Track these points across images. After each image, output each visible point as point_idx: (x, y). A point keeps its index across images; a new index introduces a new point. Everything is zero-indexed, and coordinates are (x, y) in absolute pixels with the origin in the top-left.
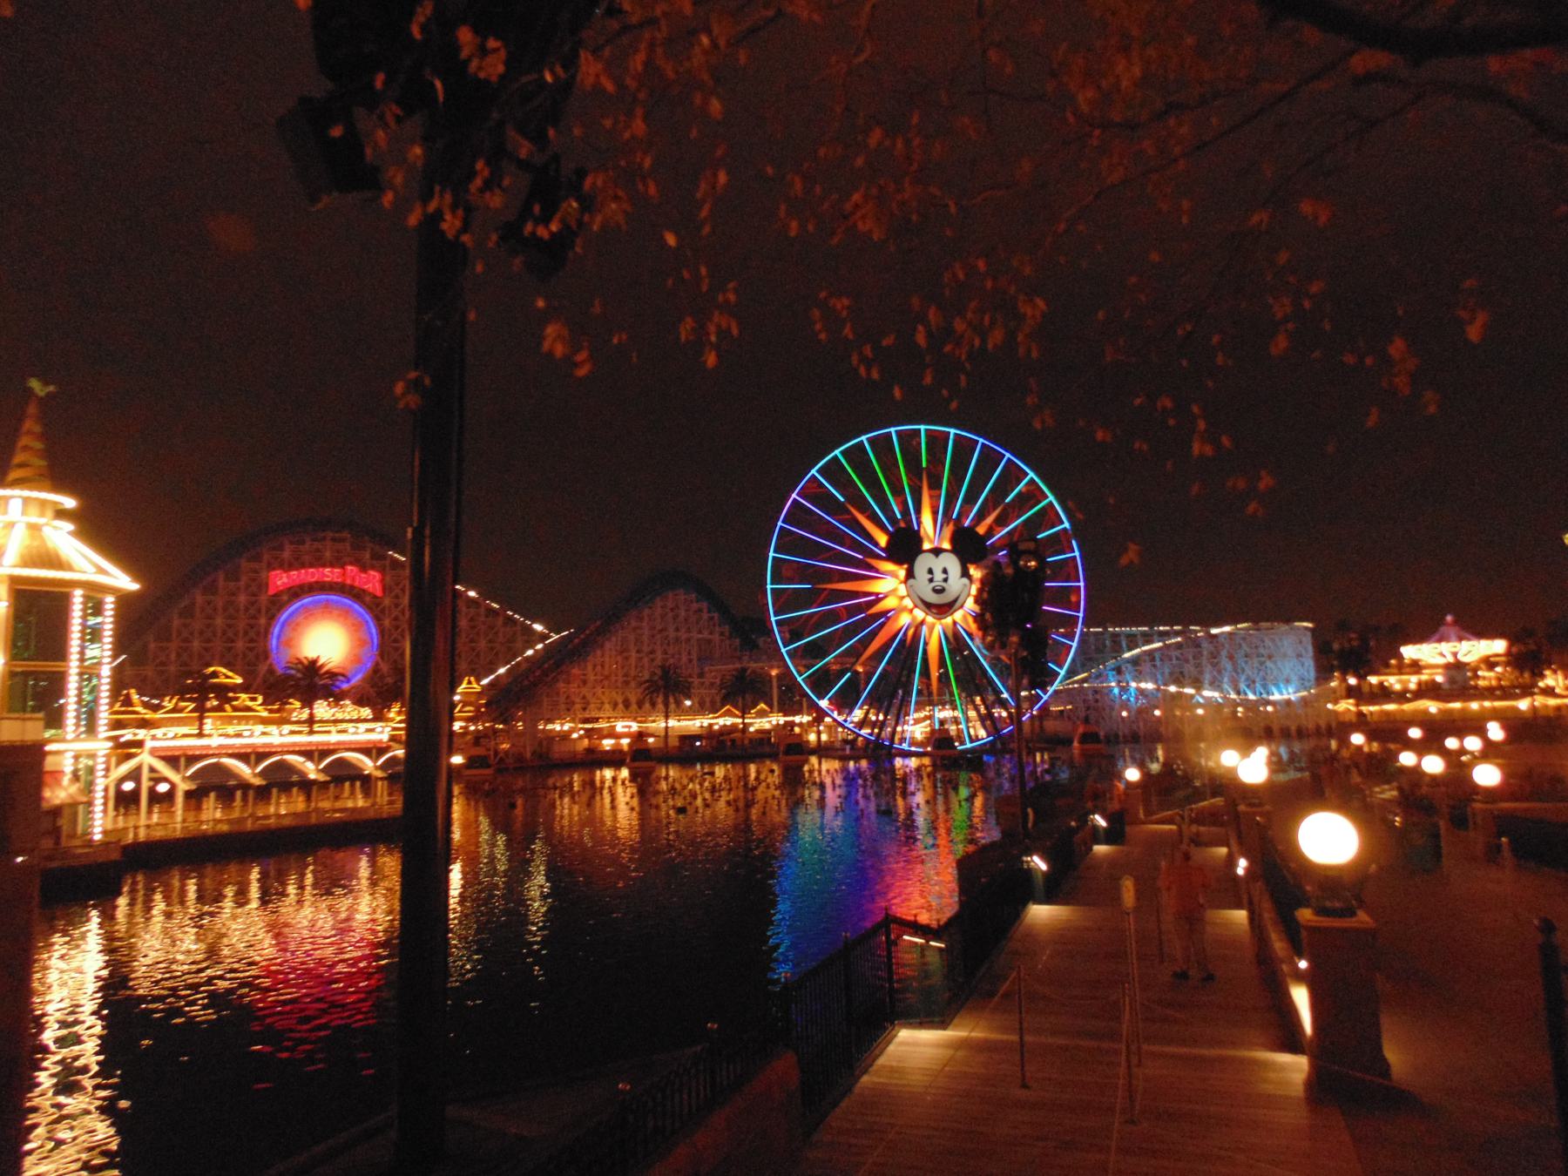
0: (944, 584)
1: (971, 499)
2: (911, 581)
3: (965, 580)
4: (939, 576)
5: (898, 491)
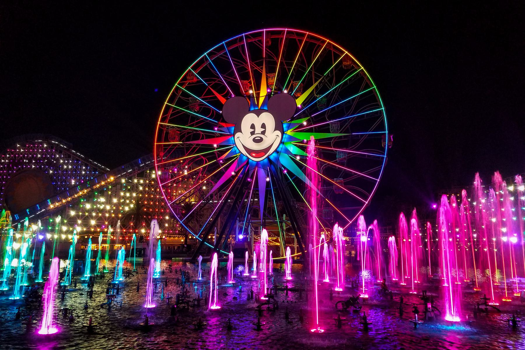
0: (262, 136)
1: (297, 76)
2: (238, 135)
3: (278, 133)
4: (259, 130)
5: (245, 76)
